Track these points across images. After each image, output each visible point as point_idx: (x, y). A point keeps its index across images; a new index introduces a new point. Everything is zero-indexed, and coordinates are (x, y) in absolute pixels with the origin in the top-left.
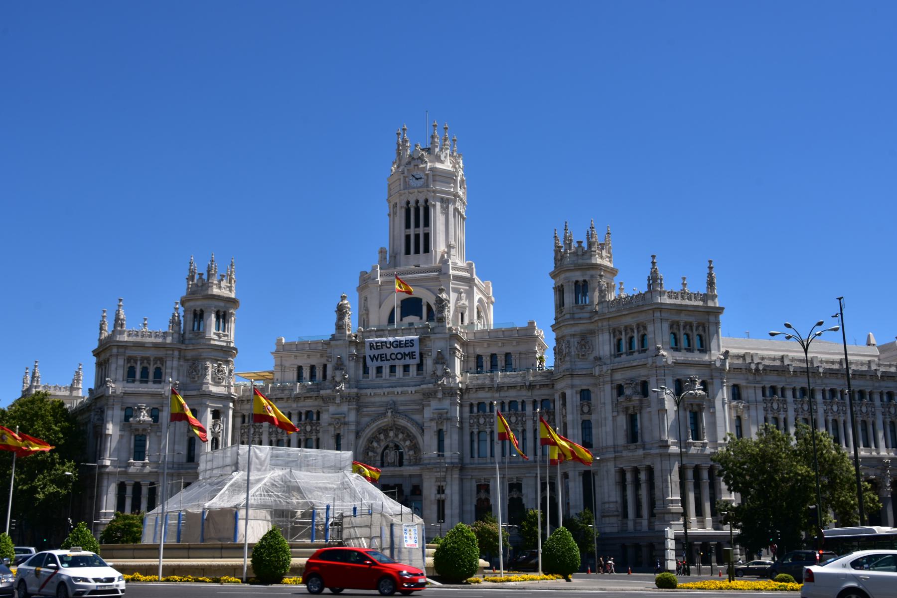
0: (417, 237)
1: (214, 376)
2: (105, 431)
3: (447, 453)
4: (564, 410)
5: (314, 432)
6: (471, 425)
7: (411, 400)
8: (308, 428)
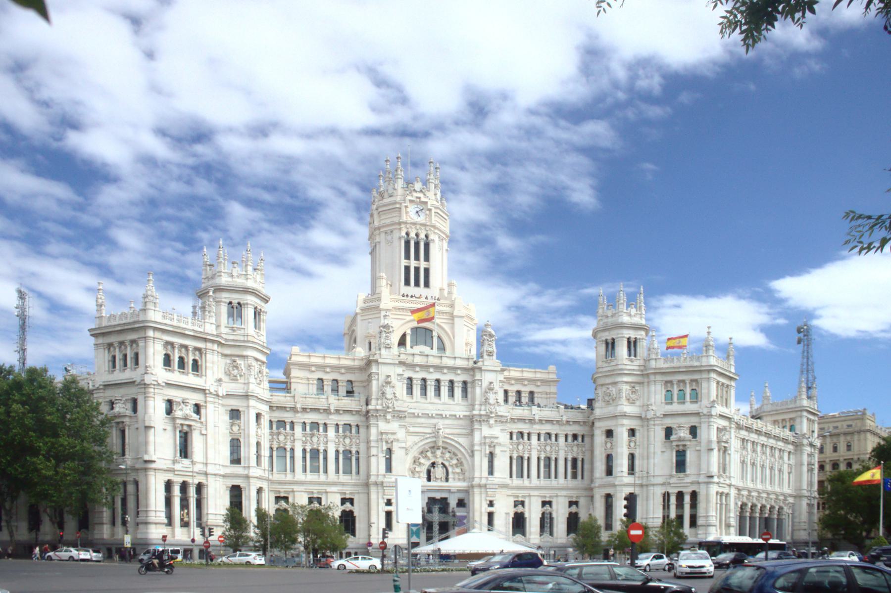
4: (609, 445)
8: (347, 441)
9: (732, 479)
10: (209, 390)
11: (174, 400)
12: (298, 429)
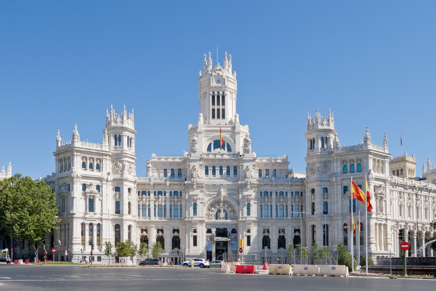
0: (218, 110)
1: (128, 170)
2: (73, 196)
3: (251, 215)
4: (313, 197)
5: (179, 202)
6: (261, 202)
7: (231, 189)
8: (176, 200)
9: (388, 215)
10: (103, 178)
11: (86, 183)
12: (152, 195)
